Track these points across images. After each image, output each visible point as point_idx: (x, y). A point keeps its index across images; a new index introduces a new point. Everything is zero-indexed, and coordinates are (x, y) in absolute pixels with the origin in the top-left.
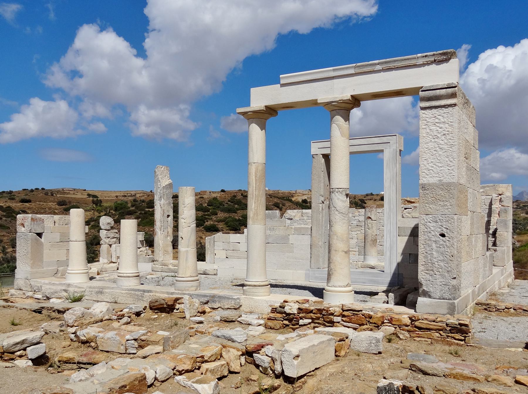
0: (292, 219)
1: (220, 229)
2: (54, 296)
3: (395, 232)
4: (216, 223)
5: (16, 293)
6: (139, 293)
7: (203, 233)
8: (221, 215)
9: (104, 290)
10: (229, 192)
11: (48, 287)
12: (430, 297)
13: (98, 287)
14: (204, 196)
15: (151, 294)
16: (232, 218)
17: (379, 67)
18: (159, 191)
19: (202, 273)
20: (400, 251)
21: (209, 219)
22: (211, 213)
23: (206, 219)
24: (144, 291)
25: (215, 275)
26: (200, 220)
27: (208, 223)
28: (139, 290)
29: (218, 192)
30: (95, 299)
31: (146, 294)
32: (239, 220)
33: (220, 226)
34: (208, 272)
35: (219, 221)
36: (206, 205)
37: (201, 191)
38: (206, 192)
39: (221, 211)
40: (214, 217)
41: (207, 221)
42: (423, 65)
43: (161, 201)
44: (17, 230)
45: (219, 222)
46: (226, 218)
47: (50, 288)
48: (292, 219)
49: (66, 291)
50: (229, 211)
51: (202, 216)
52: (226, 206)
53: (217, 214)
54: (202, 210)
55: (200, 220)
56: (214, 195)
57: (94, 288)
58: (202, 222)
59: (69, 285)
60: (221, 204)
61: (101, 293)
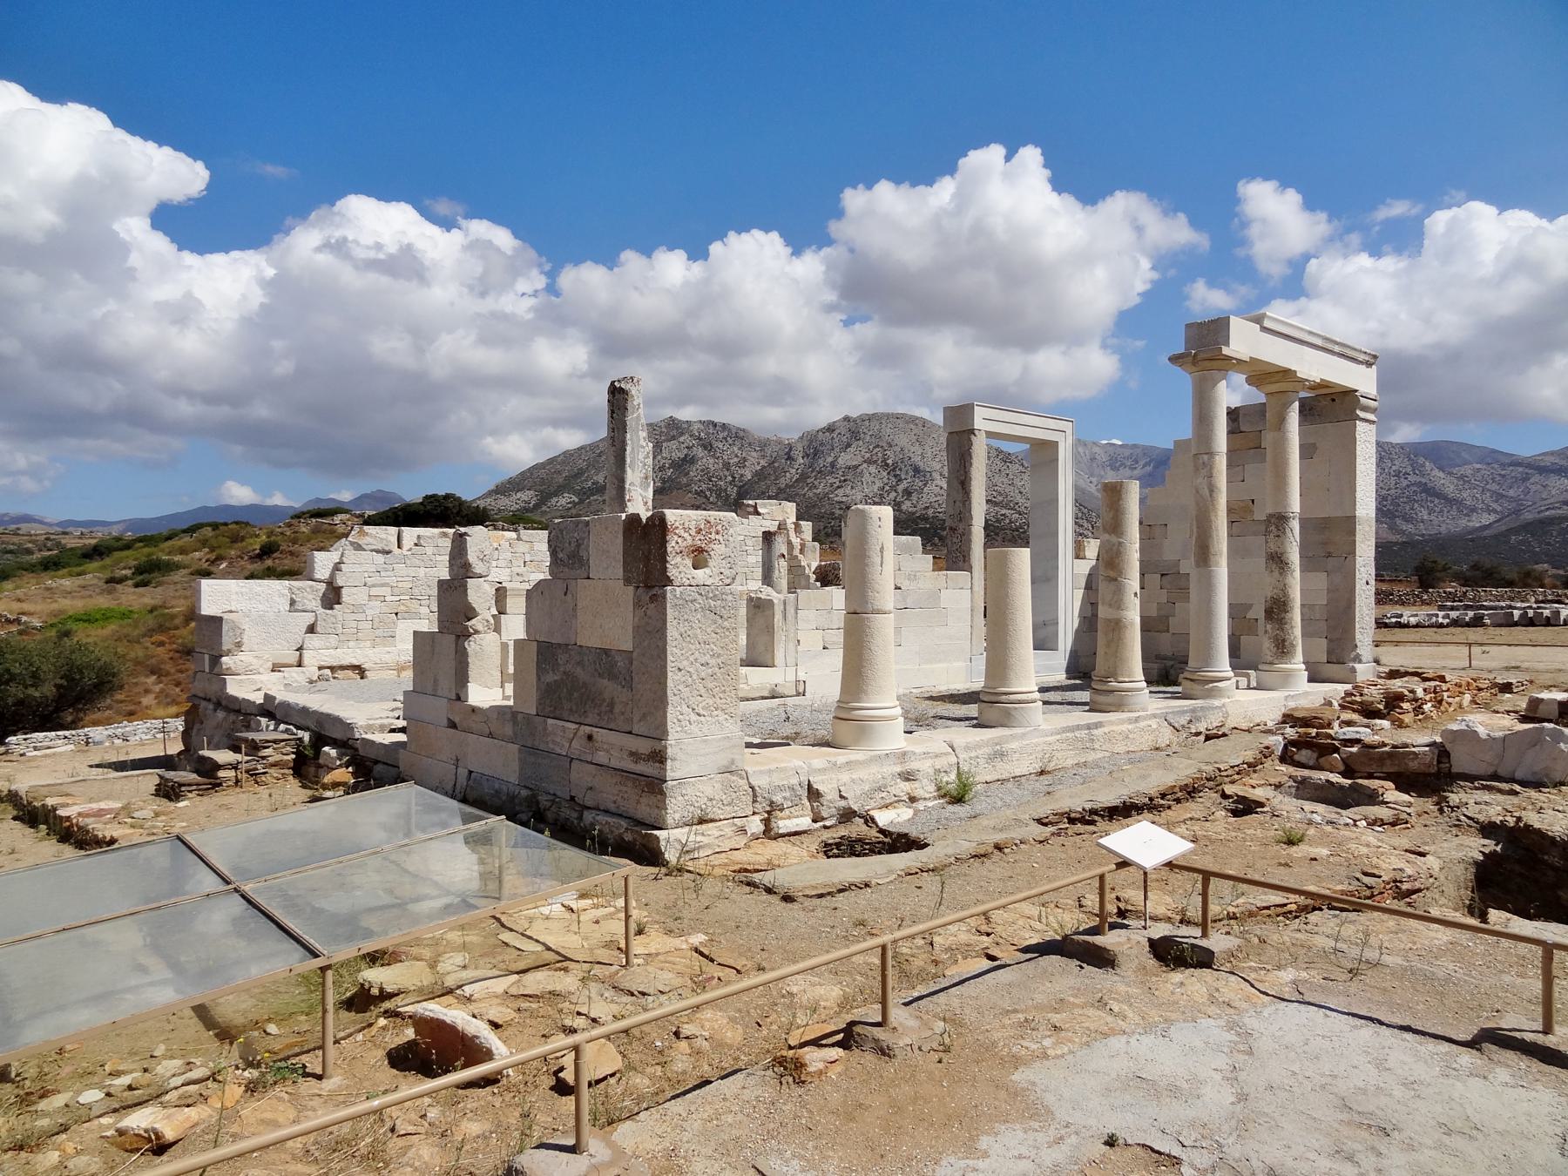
0: (388, 552)
2: (873, 805)
3: (1069, 585)
5: (705, 840)
6: (1083, 734)
9: (1006, 747)
11: (845, 777)
12: (1360, 662)
13: (987, 743)
15: (1106, 729)
17: (1337, 349)
18: (641, 457)
19: (766, 694)
20: (1076, 613)
24: (1089, 727)
25: (798, 694)
28: (1078, 727)
30: (989, 779)
31: (1095, 732)
34: (780, 690)
42: (1361, 363)
43: (646, 489)
44: (672, 572)
47: (853, 781)
48: (388, 552)
49: (908, 777)
57: (978, 746)
59: (903, 756)
61: (1001, 755)
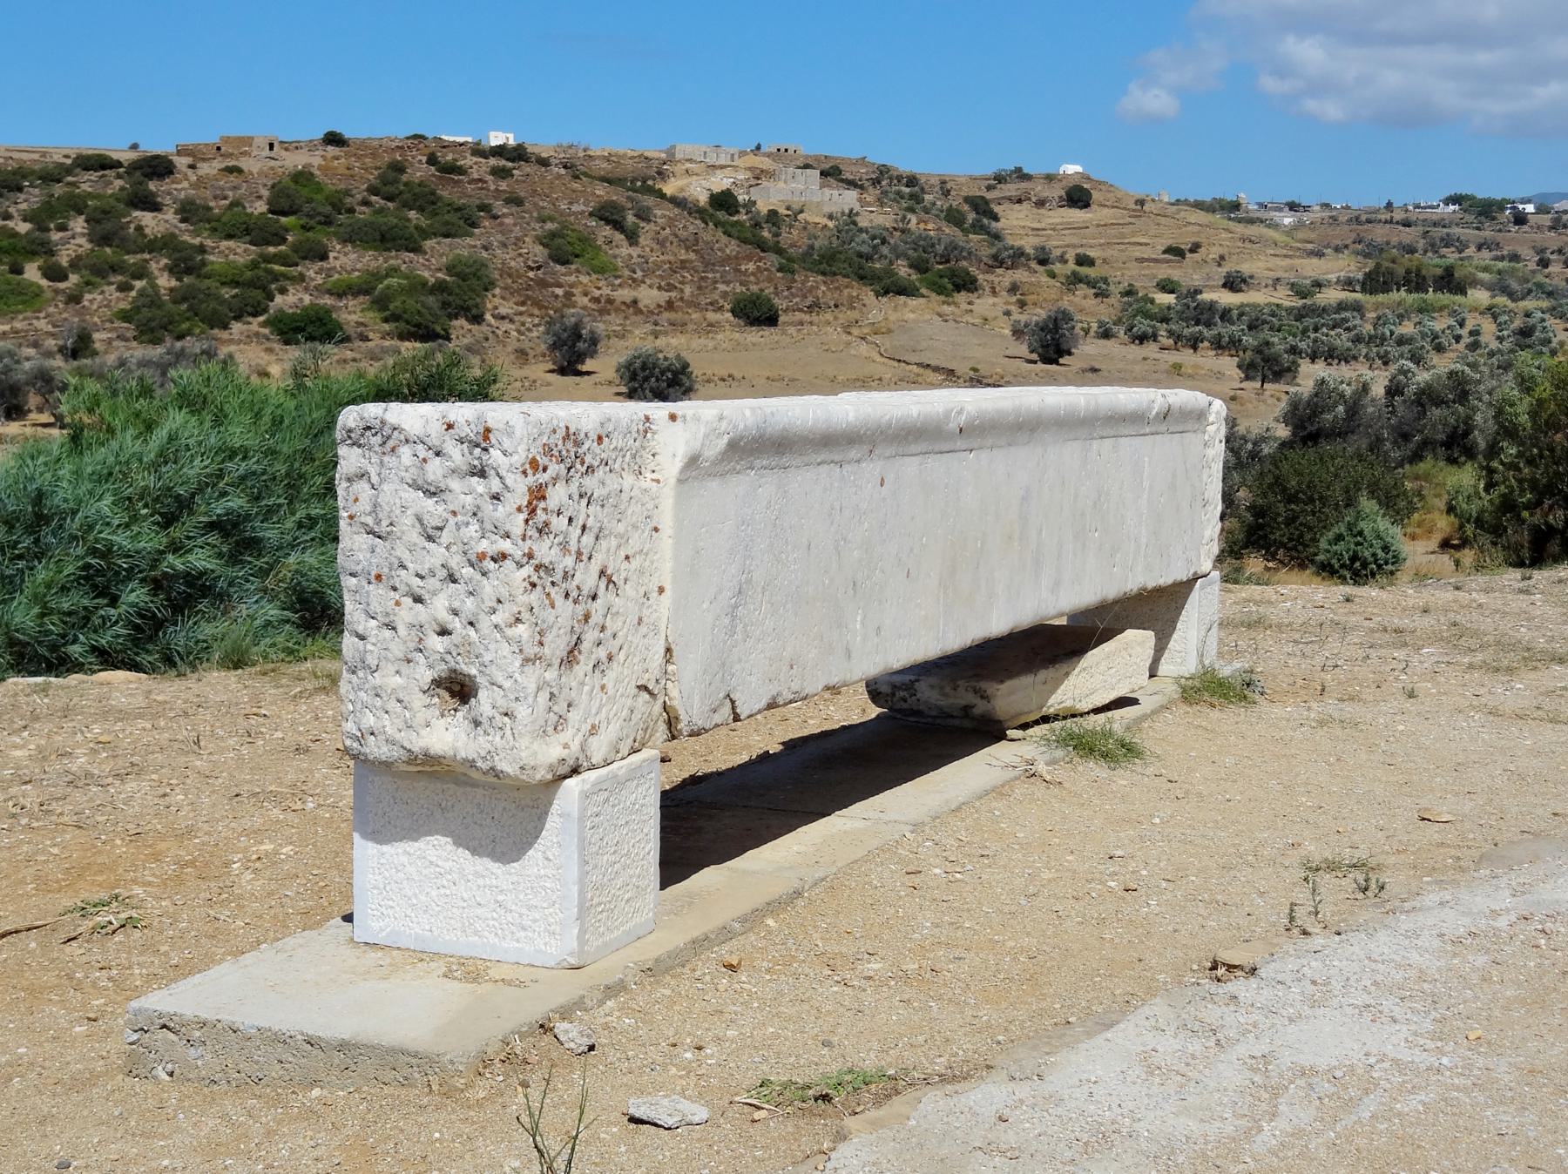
1: (351, 331)
4: (328, 301)
7: (270, 350)
8: (347, 261)
10: (364, 144)
14: (244, 163)
16: (406, 277)
21: (292, 279)
22: (296, 248)
23: (276, 277)
26: (252, 284)
27: (289, 301)
29: (311, 146)
32: (441, 287)
33: (351, 313)
35: (340, 292)
36: (260, 207)
37: (226, 140)
38: (249, 141)
39: (344, 242)
40: (311, 271)
41: (283, 291)
45: (340, 296)
46: (377, 277)
50: (386, 239)
51: (254, 265)
52: (363, 214)
53: (324, 257)
54: (248, 231)
55: (252, 284)
56: (295, 161)
58: (258, 294)
60: (338, 203)
